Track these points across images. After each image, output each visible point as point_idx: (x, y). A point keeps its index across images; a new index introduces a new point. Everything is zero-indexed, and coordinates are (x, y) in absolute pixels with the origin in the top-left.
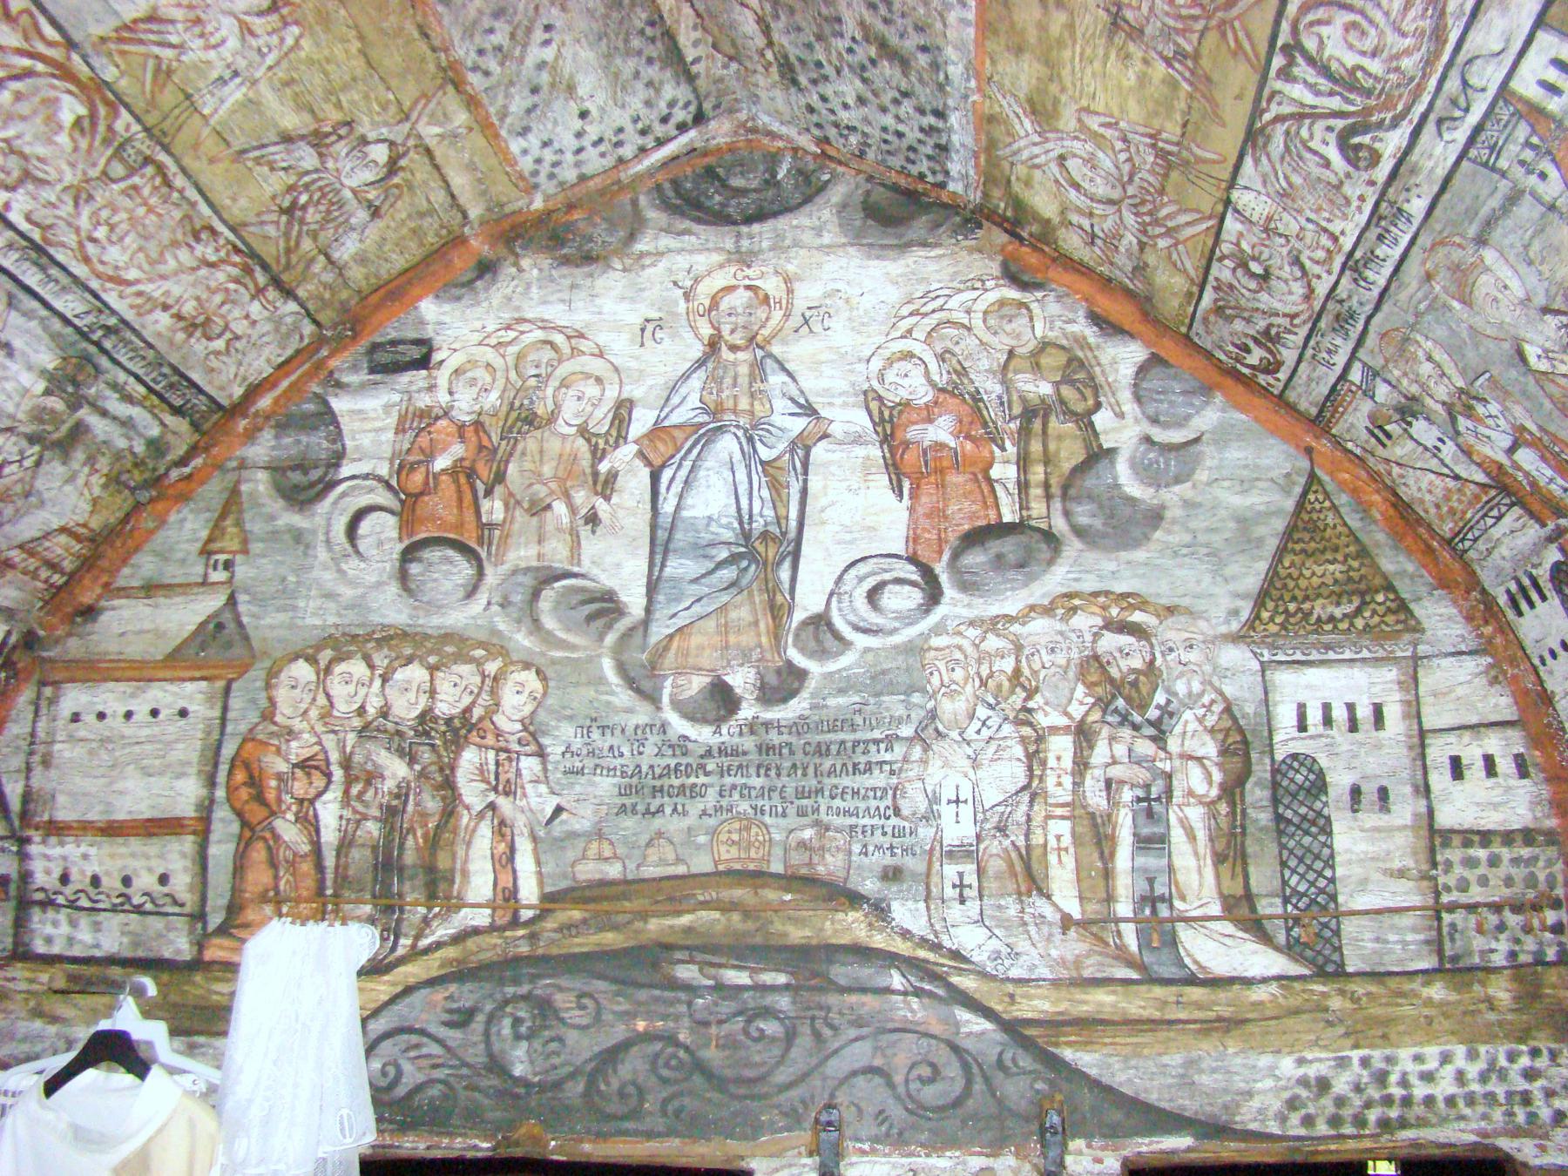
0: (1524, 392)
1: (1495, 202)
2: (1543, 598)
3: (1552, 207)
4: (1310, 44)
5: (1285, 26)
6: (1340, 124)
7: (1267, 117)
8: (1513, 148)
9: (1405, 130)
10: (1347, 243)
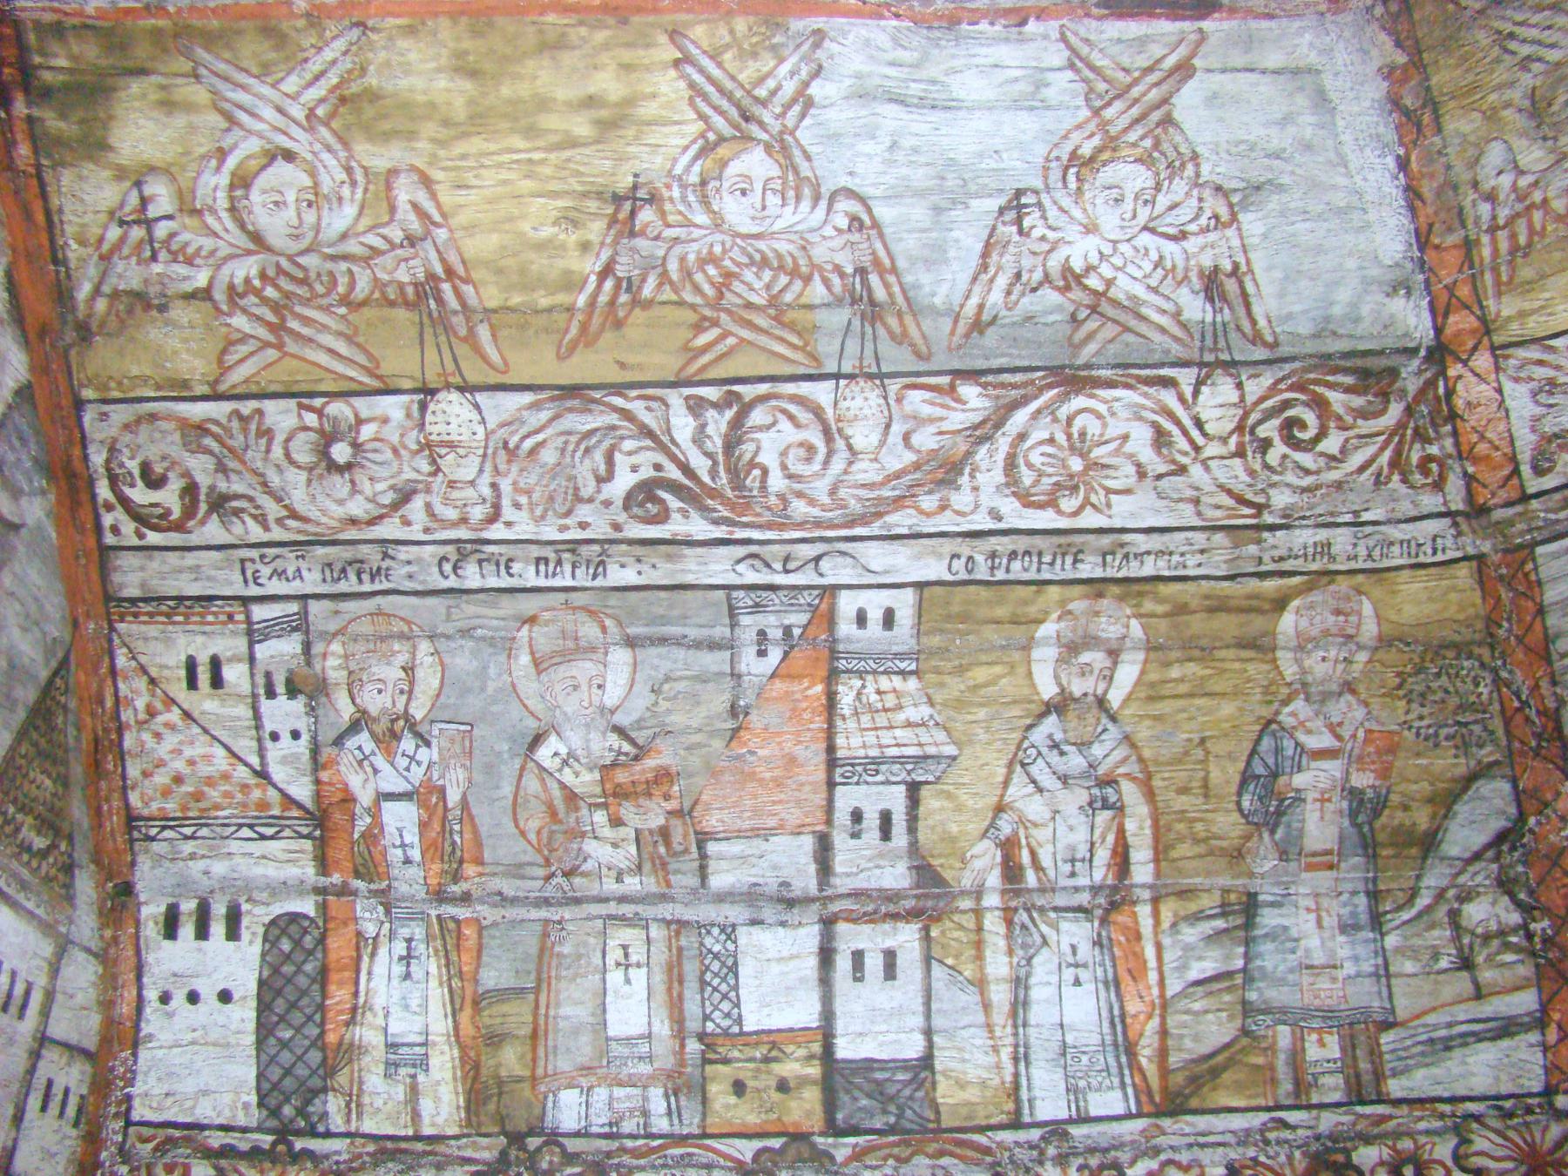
0: (489, 769)
1: (693, 633)
2: (233, 934)
3: (736, 676)
4: (758, 416)
5: (763, 388)
6: (673, 473)
7: (618, 401)
8: (772, 619)
9: (720, 532)
10: (497, 532)
